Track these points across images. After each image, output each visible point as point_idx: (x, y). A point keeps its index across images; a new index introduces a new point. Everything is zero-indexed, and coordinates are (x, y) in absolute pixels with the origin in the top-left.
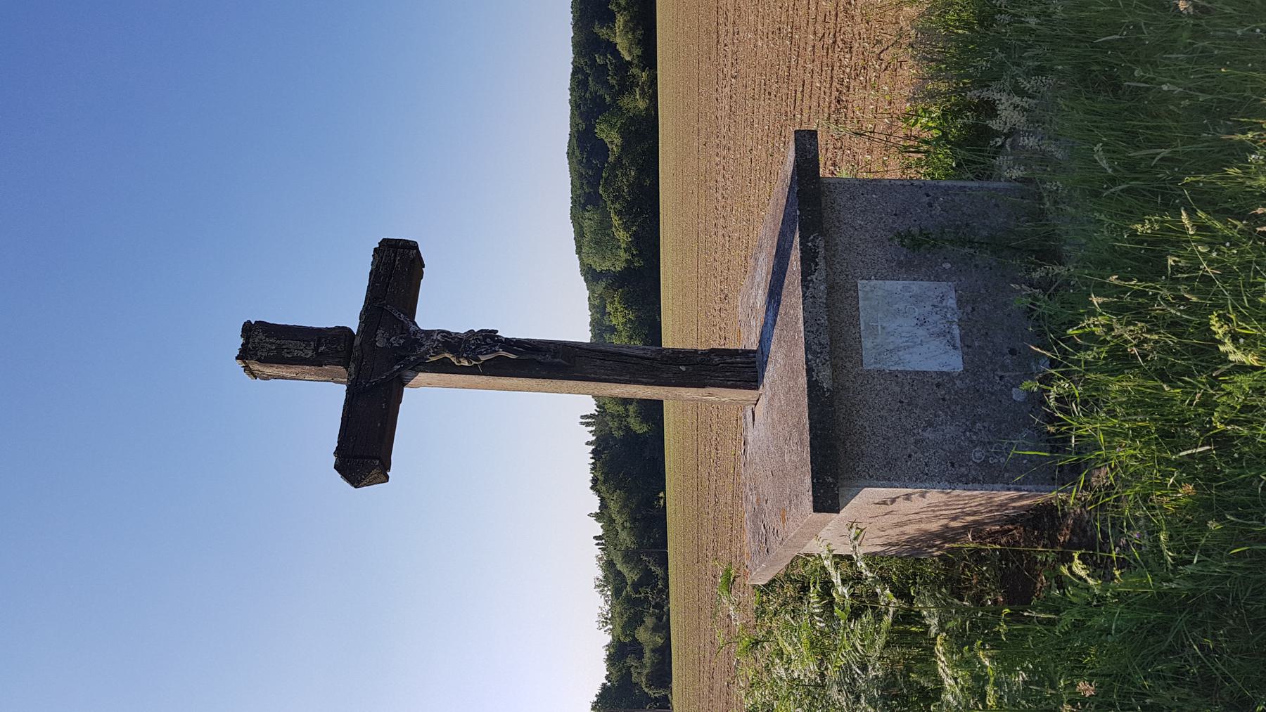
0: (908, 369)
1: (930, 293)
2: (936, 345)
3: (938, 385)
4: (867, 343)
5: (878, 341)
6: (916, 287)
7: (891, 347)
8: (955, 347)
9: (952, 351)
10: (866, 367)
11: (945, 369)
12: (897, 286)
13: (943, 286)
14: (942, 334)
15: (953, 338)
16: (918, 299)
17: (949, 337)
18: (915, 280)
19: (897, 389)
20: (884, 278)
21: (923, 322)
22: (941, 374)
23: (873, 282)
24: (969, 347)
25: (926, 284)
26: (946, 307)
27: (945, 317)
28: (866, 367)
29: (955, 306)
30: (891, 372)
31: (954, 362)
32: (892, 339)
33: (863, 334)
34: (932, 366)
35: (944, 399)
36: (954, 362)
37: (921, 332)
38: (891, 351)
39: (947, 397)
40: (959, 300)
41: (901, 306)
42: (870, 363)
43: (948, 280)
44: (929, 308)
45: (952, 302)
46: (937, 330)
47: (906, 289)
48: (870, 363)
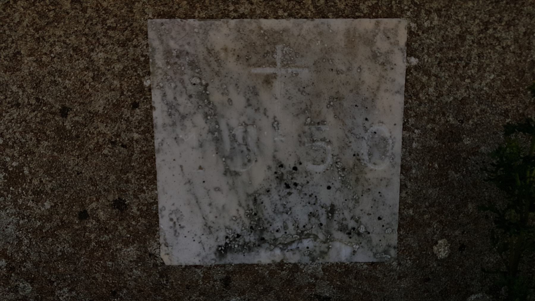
0: (159, 136)
1: (366, 203)
2: (229, 208)
3: (120, 205)
4: (223, 34)
5: (231, 65)
6: (385, 171)
7: (216, 97)
8: (223, 250)
9: (211, 243)
10: (155, 28)
11: (164, 224)
12: (389, 119)
13: (385, 237)
14: (257, 224)
15: (247, 248)
16: (350, 173)
17: (251, 238)
18: (405, 169)
19: (99, 105)
20: (411, 90)
21: (286, 178)
22: (151, 213)
23: (400, 62)
24: (227, 282)
25: (393, 195)
26: (329, 239)
27: (303, 234)
28: (155, 28)
29: (332, 258)
30: (145, 93)
31: (185, 246)
32: (239, 100)
33: (250, 24)
34: (171, 193)
35: (83, 215)
36: (185, 246)
37: (259, 174)
38: (204, 95)
39: (91, 224)
40: (346, 270)
41: (332, 129)
42: (166, 37)
43: (403, 247)
44: (325, 197)
45: (342, 251)
46: (268, 211)
47: (380, 144)
48: (166, 37)
